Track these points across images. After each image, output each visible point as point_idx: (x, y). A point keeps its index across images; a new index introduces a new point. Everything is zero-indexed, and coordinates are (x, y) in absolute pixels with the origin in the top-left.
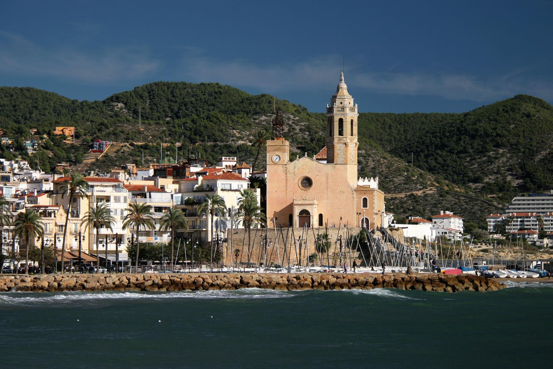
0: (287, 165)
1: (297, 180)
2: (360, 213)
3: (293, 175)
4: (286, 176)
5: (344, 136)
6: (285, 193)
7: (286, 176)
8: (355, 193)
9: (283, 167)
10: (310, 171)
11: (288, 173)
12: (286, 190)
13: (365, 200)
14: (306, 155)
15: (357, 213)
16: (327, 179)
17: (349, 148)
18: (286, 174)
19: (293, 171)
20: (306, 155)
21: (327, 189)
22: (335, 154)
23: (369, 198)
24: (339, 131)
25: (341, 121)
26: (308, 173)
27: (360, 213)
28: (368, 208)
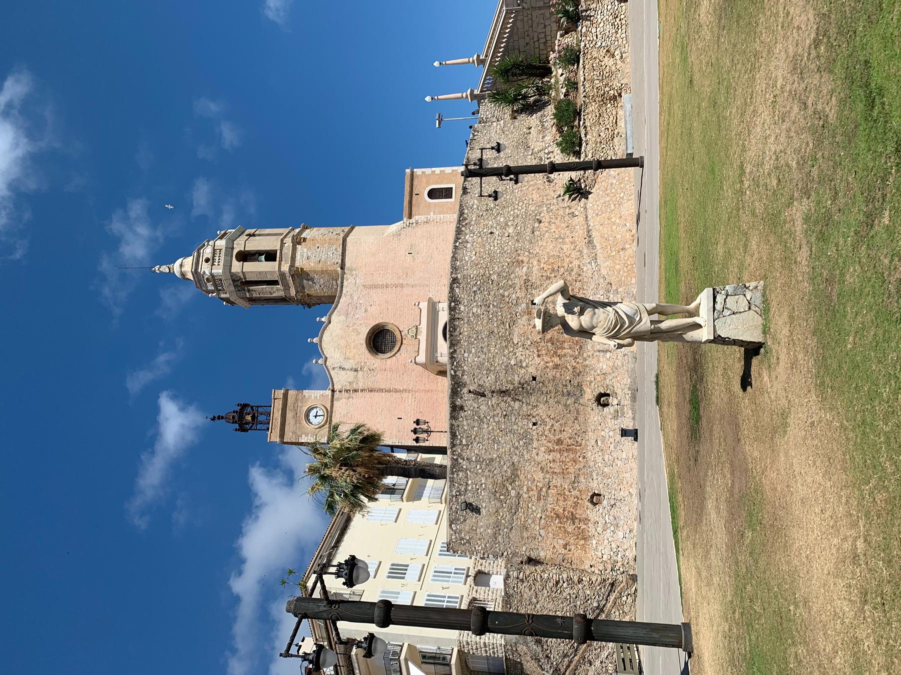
1: (376, 361)
3: (360, 373)
4: (362, 391)
6: (405, 395)
7: (362, 391)
9: (338, 399)
11: (355, 386)
12: (396, 391)
13: (433, 194)
14: (315, 340)
16: (376, 287)
18: (356, 391)
19: (353, 373)
20: (315, 340)
21: (402, 286)
22: (319, 267)
23: (428, 184)
24: (267, 260)
25: (245, 256)
26: (359, 334)
28: (453, 186)
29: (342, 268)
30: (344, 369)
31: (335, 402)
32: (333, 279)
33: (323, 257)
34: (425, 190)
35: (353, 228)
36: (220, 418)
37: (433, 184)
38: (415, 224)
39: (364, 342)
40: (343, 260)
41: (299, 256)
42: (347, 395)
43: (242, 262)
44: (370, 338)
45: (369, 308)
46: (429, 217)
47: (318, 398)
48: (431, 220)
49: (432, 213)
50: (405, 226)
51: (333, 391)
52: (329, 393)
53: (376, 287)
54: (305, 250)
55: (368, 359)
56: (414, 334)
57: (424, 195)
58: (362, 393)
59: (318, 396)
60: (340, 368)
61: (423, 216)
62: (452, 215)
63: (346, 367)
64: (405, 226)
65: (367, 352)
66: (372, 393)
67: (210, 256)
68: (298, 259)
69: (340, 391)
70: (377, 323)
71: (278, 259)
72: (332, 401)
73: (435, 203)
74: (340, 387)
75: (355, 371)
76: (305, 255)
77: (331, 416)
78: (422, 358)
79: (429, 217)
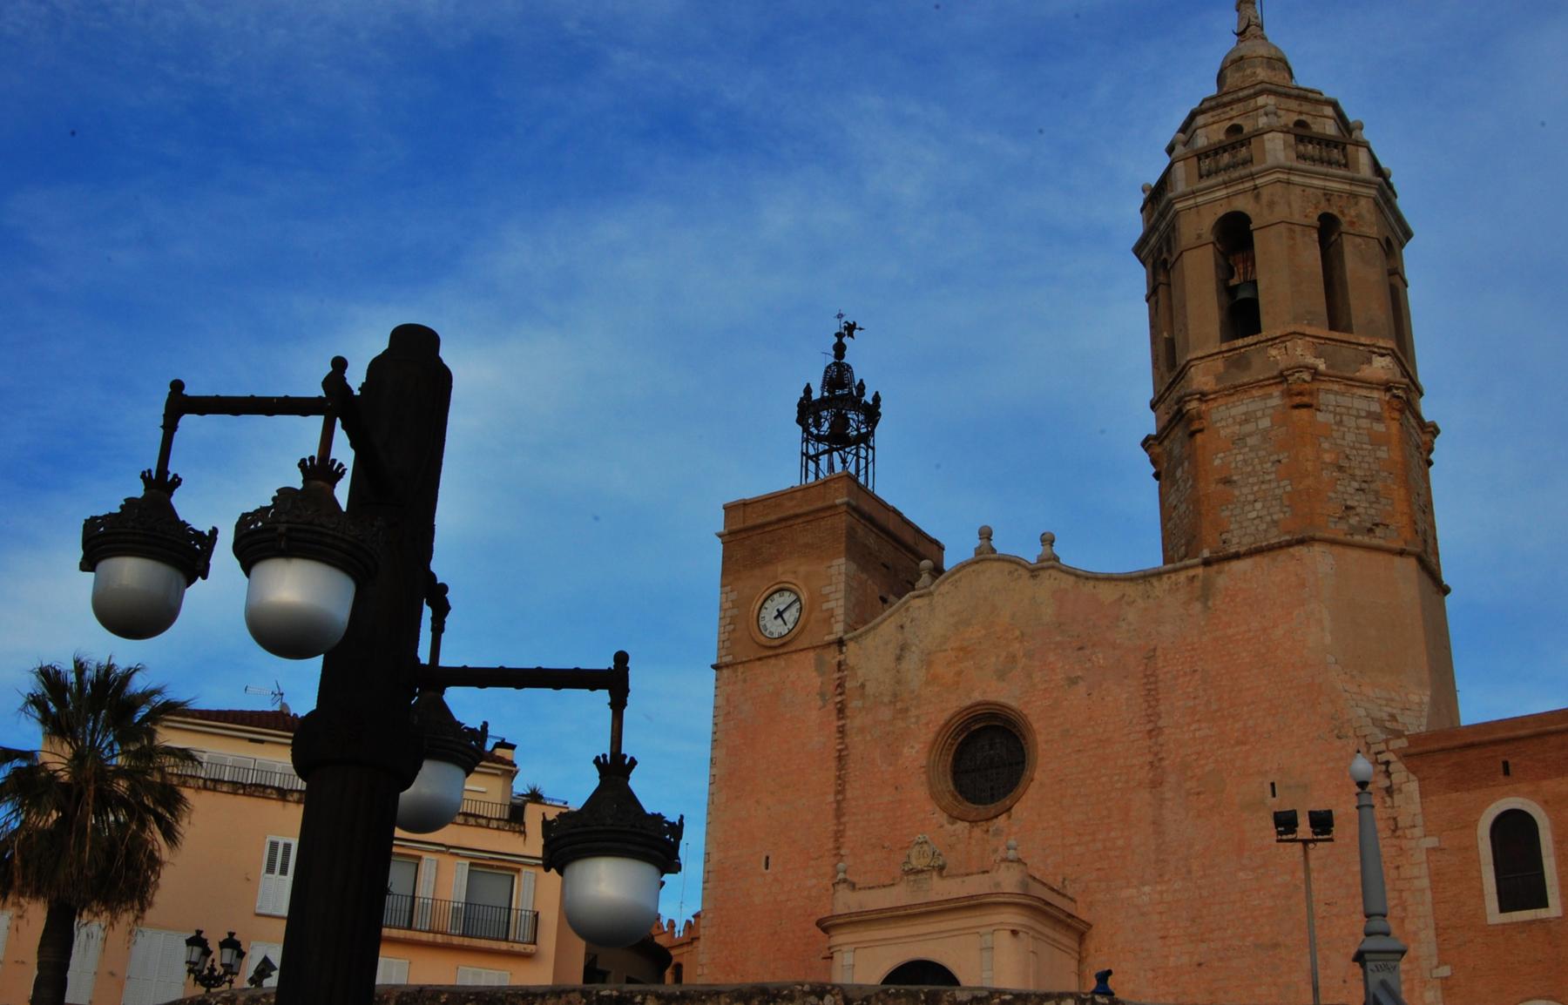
0: (851, 648)
1: (917, 751)
2: (1323, 823)
3: (886, 714)
4: (842, 731)
5: (1264, 335)
7: (842, 731)
8: (1413, 787)
9: (820, 665)
10: (1012, 659)
11: (855, 704)
12: (838, 836)
15: (1285, 822)
16: (1152, 692)
17: (1320, 417)
18: (841, 711)
21: (1156, 784)
26: (1001, 675)
27: (1323, 823)
28: (1554, 909)
29: (1207, 563)
30: (899, 659)
31: (812, 654)
32: (1188, 544)
33: (1245, 490)
34: (1528, 795)
35: (1401, 553)
36: (840, 349)
37: (1556, 826)
38: (1387, 783)
39: (977, 697)
40: (1237, 556)
41: (1243, 409)
42: (832, 688)
43: (1212, 238)
44: (994, 716)
45: (1082, 688)
46: (1418, 832)
47: (825, 606)
48: (1404, 843)
49: (1432, 842)
50: (1375, 748)
51: (840, 643)
52: (838, 629)
53: (1152, 692)
54: (1265, 423)
55: (927, 724)
56: (916, 863)
57: (1507, 795)
58: (834, 729)
59: (832, 604)
60: (903, 648)
61: (1416, 807)
62: (1431, 922)
63: (904, 665)
64: (1372, 751)
65: (946, 715)
66: (833, 764)
67: (1248, 128)
68: (1234, 411)
69: (840, 664)
70: (1036, 726)
71: (1225, 347)
72: (814, 648)
73: (1475, 847)
74: (851, 661)
75: (895, 695)
76: (1249, 428)
77: (777, 656)
78: (846, 901)
79: (1418, 832)
